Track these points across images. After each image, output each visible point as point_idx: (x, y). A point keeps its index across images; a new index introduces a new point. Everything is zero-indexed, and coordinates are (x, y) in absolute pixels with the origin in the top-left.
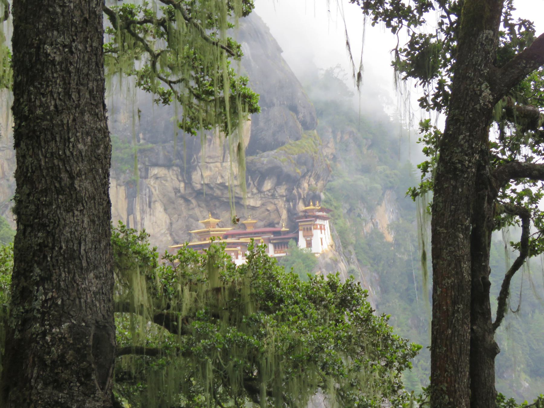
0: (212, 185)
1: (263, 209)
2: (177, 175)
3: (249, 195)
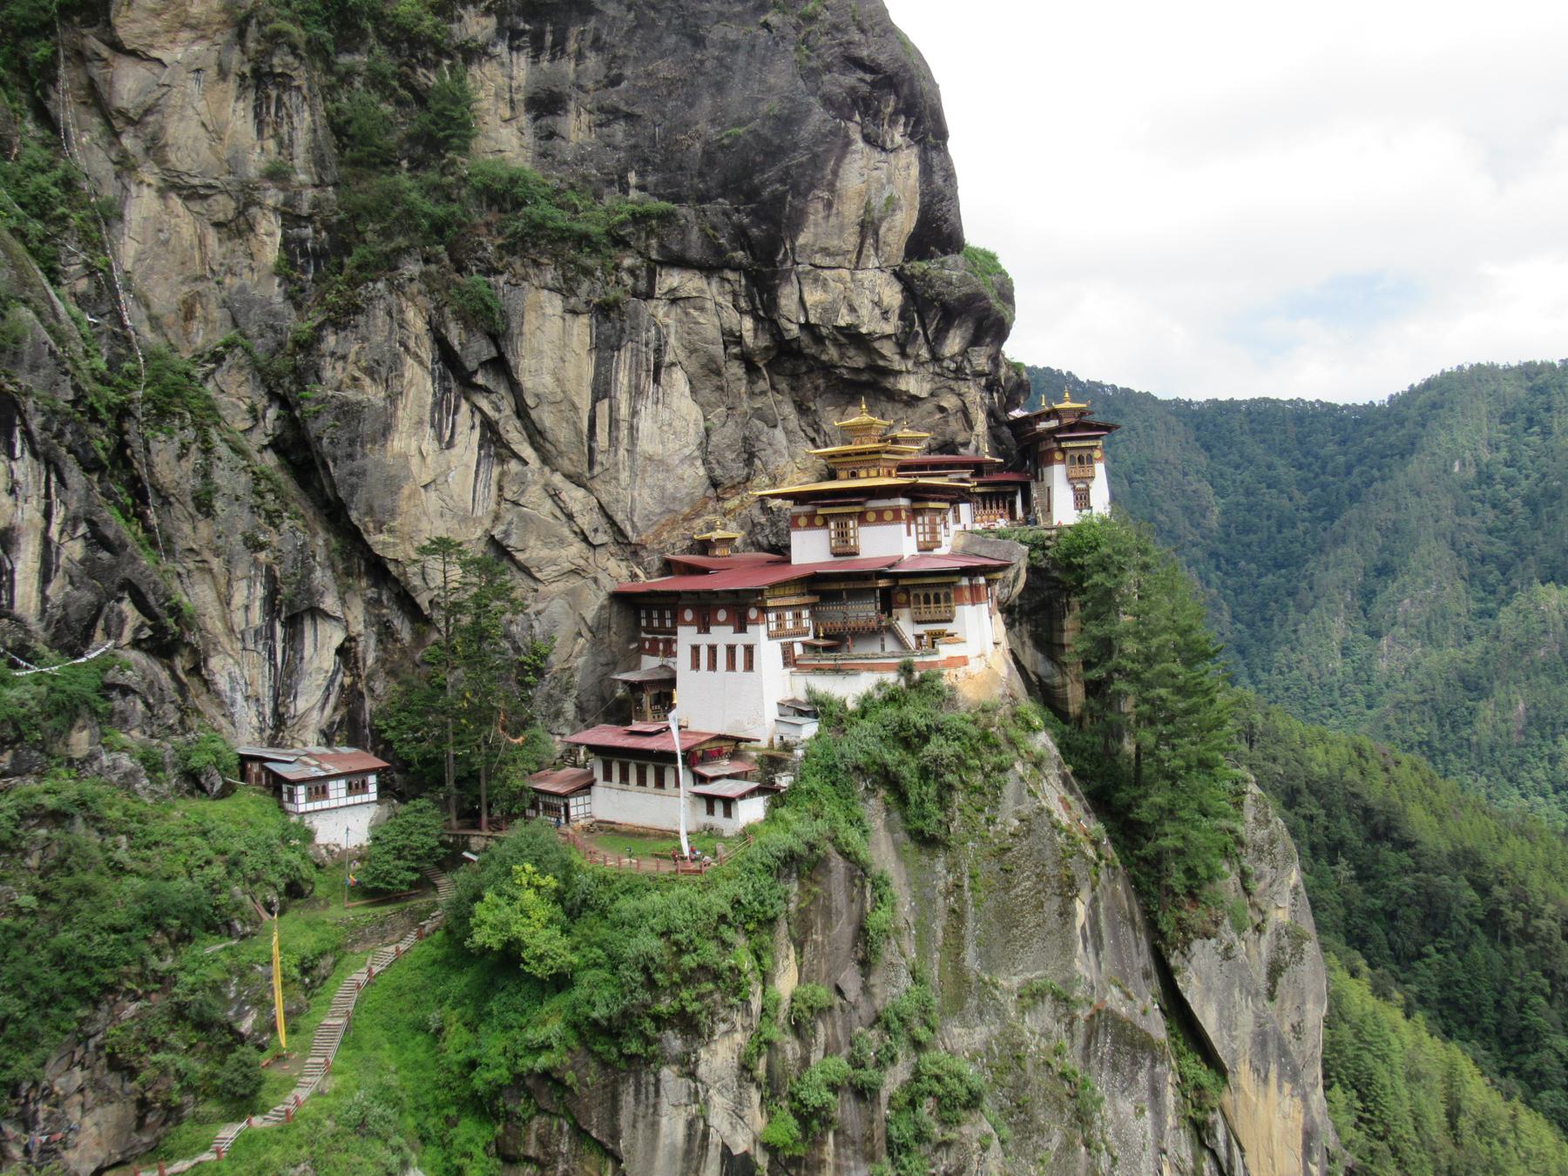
0: (824, 331)
1: (929, 406)
2: (735, 294)
3: (910, 364)
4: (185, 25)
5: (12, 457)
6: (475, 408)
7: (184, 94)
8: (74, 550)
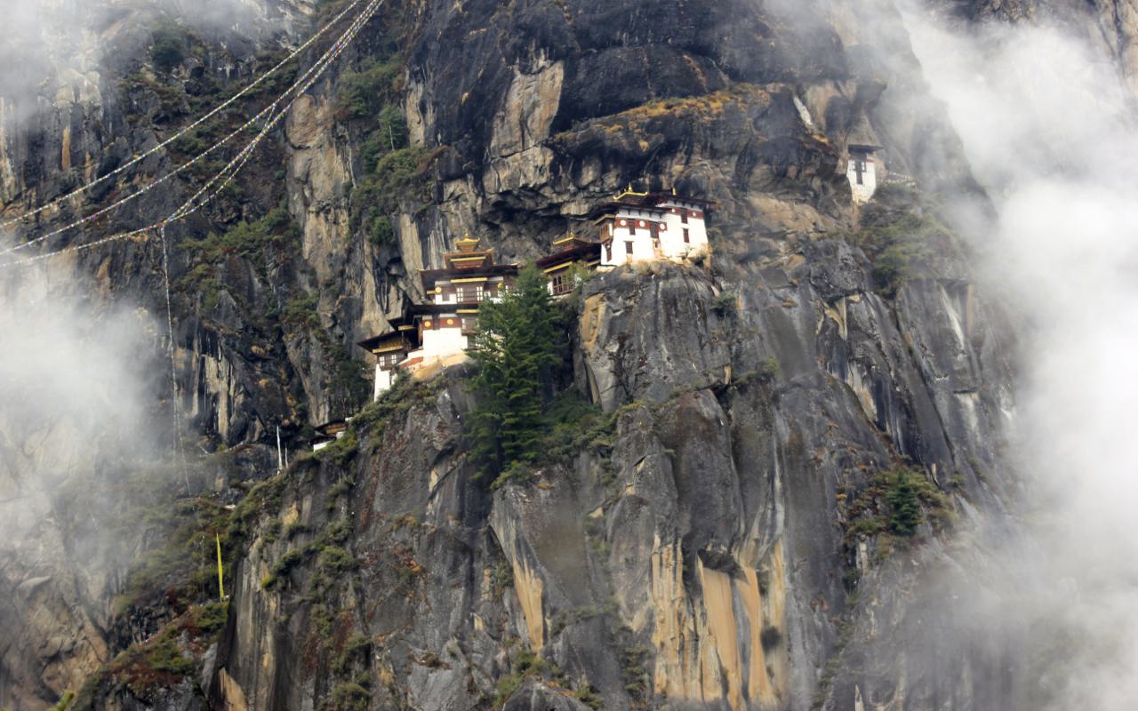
3: (566, 197)
4: (318, 125)
5: (219, 361)
6: (398, 289)
7: (317, 161)
8: (240, 399)
